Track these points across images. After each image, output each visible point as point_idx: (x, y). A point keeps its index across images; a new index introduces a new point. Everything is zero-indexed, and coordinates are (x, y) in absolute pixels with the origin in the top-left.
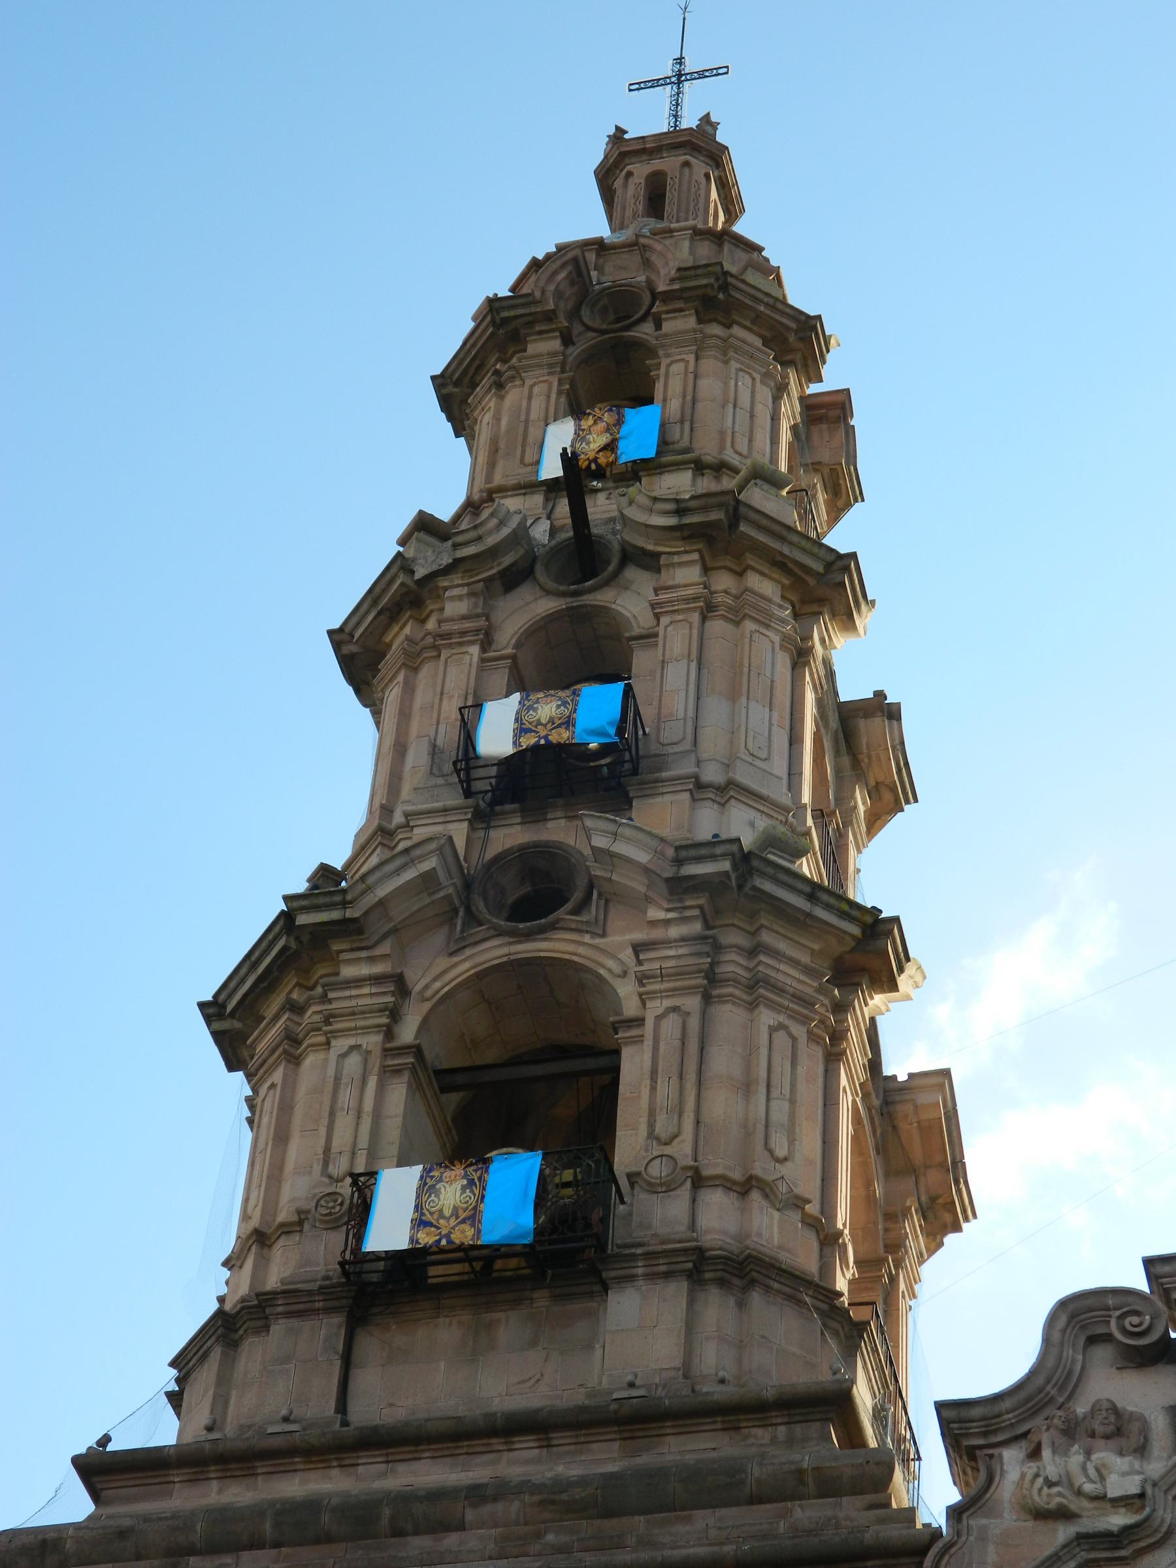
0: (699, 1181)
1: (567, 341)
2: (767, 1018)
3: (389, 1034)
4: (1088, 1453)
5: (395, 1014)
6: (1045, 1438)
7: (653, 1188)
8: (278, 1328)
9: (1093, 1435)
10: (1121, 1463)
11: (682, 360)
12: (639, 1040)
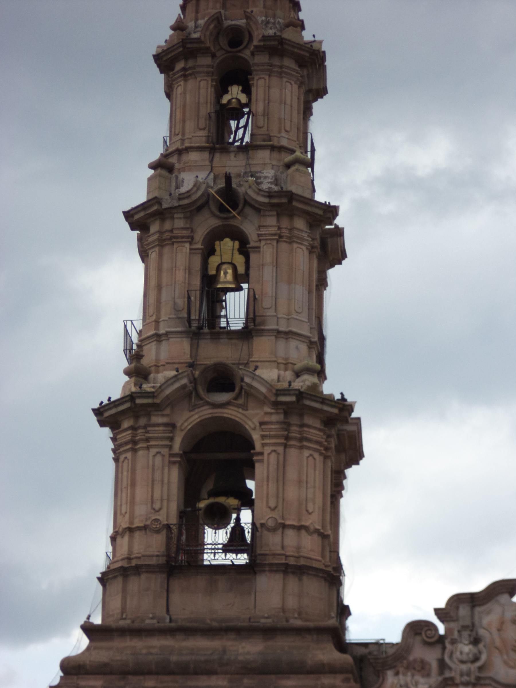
0: (284, 526)
1: (213, 56)
2: (306, 453)
3: (170, 447)
4: (413, 676)
5: (171, 439)
6: (401, 670)
7: (269, 530)
8: (144, 576)
9: (414, 669)
10: (422, 680)
11: (263, 78)
12: (262, 461)
